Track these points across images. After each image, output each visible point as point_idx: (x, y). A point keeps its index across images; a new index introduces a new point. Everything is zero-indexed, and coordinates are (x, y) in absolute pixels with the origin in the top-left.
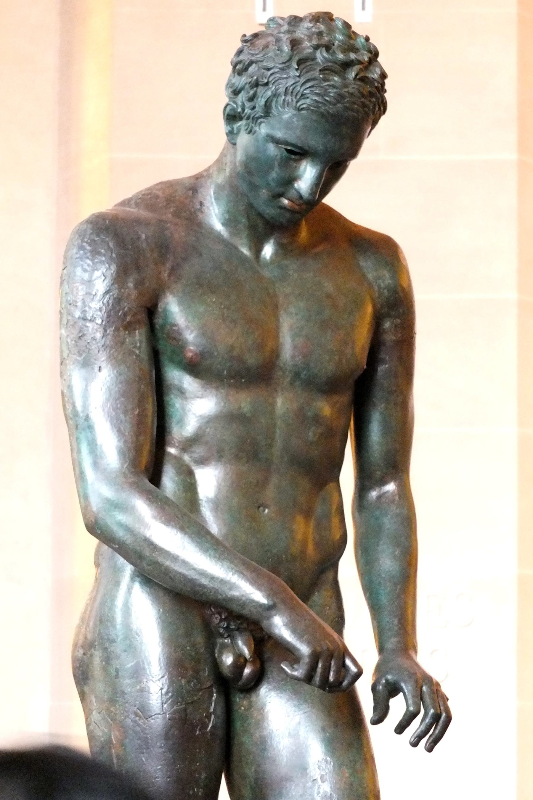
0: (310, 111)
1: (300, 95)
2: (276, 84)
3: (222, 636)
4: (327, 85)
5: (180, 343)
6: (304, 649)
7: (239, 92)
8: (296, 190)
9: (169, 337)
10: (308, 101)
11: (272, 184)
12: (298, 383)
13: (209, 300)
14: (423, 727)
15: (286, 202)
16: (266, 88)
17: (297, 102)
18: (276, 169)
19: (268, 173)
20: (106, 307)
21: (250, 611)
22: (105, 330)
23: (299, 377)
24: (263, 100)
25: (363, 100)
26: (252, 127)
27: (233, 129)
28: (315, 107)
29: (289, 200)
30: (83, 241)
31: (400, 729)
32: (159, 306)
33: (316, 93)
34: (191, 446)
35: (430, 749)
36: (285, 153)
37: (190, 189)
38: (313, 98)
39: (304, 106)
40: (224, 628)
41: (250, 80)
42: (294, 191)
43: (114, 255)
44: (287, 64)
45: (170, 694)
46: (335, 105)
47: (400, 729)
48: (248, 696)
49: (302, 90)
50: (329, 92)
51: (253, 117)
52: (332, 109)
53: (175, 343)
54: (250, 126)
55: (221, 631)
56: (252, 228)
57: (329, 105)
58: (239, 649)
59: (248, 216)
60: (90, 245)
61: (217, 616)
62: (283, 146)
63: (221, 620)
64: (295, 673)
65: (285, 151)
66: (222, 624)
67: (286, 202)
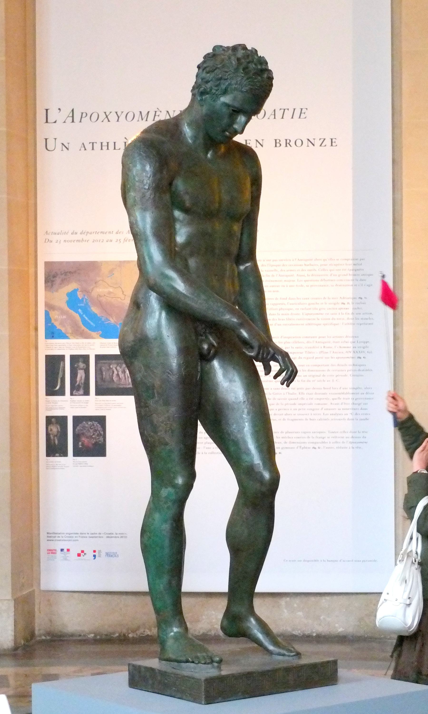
3: (202, 336)
6: (255, 344)
7: (209, 82)
8: (234, 128)
14: (287, 376)
15: (227, 133)
31: (275, 377)
35: (288, 386)
39: (245, 90)
45: (185, 364)
46: (259, 90)
47: (275, 377)
49: (245, 83)
55: (202, 333)
63: (202, 329)
64: (252, 354)
67: (227, 133)
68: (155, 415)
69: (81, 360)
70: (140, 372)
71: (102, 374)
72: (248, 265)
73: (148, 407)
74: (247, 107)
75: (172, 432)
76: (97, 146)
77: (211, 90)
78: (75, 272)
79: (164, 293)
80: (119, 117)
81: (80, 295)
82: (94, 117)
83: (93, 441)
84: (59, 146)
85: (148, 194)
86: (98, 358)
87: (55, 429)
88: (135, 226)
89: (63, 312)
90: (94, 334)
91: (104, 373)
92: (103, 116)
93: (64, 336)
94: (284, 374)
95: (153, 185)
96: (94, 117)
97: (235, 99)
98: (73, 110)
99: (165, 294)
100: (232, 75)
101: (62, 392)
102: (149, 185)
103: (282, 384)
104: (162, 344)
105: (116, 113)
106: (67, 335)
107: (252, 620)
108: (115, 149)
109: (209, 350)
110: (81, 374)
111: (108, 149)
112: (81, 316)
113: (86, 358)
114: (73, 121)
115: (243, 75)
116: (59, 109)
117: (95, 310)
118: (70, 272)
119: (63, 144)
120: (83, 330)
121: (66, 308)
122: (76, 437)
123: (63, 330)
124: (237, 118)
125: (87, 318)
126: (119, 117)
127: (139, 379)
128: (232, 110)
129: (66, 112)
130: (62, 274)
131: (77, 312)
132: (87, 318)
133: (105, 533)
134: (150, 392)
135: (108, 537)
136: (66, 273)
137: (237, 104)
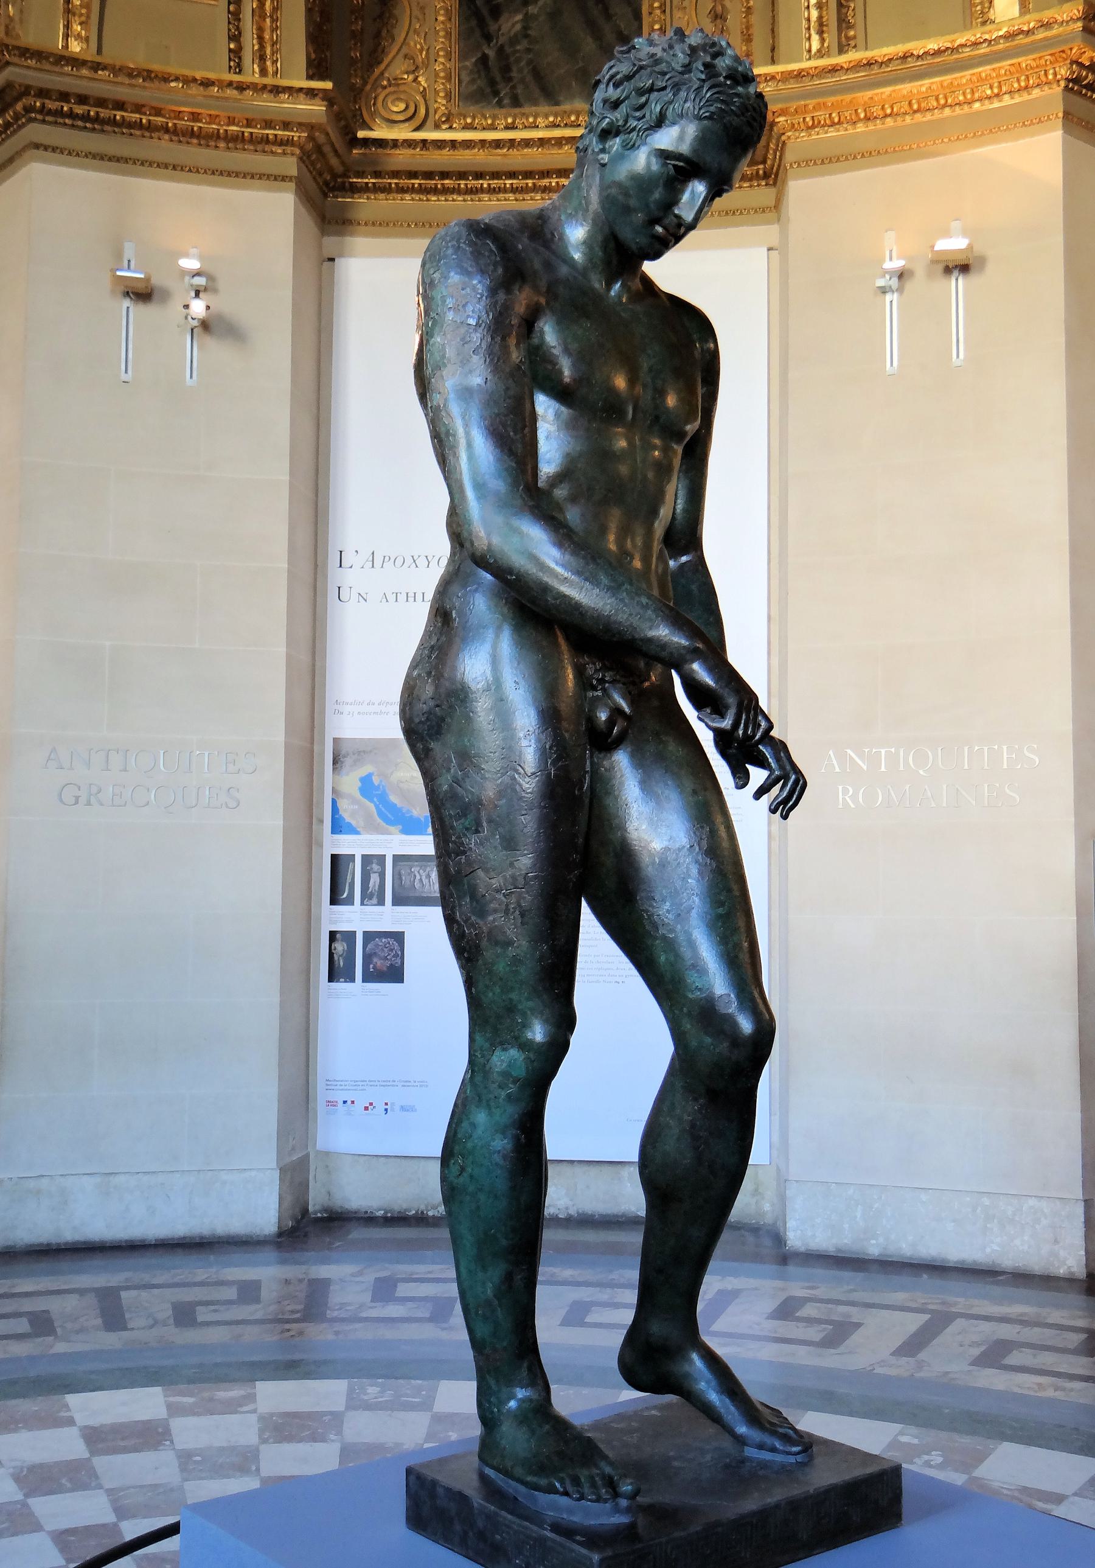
3: (594, 688)
7: (623, 101)
8: (678, 217)
11: (652, 206)
14: (785, 794)
17: (700, 109)
18: (660, 189)
19: (651, 192)
21: (671, 653)
22: (493, 338)
29: (664, 228)
30: (458, 241)
31: (759, 794)
35: (785, 817)
36: (672, 171)
39: (707, 114)
40: (598, 680)
41: (642, 85)
42: (673, 218)
43: (498, 259)
44: (688, 68)
46: (738, 116)
47: (759, 794)
48: (609, 755)
49: (708, 95)
52: (736, 121)
54: (633, 141)
55: (595, 682)
56: (607, 263)
58: (614, 702)
59: (605, 248)
60: (470, 246)
61: (590, 666)
62: (673, 162)
63: (596, 671)
66: (596, 676)
68: (480, 873)
69: (375, 861)
70: (449, 770)
71: (400, 879)
72: (684, 559)
73: (464, 853)
74: (712, 159)
75: (522, 915)
76: (402, 598)
77: (626, 121)
78: (371, 751)
79: (510, 571)
80: (429, 562)
81: (376, 780)
82: (399, 562)
83: (388, 963)
84: (355, 596)
85: (476, 337)
86: (397, 859)
87: (340, 947)
88: (443, 413)
89: (355, 801)
90: (392, 829)
91: (404, 878)
92: (409, 561)
93: (353, 831)
94: (776, 790)
95: (488, 315)
96: (399, 562)
97: (681, 138)
98: (373, 553)
99: (511, 575)
100: (676, 80)
101: (350, 901)
102: (479, 318)
103: (773, 811)
104: (502, 700)
105: (426, 557)
106: (358, 829)
107: (695, 1357)
108: (423, 600)
109: (611, 722)
110: (374, 879)
111: (415, 601)
112: (377, 806)
113: (381, 859)
114: (373, 567)
115: (703, 77)
116: (357, 551)
117: (393, 799)
118: (364, 752)
119: (359, 594)
120: (379, 824)
121: (358, 795)
122: (367, 958)
123: (354, 823)
124: (682, 191)
125: (383, 809)
126: (429, 562)
127: (445, 787)
128: (674, 166)
129: (365, 555)
130: (354, 754)
131: (372, 801)
132: (383, 809)
133: (400, 1081)
134: (471, 817)
135: (403, 1086)
136: (359, 752)
137: (685, 148)
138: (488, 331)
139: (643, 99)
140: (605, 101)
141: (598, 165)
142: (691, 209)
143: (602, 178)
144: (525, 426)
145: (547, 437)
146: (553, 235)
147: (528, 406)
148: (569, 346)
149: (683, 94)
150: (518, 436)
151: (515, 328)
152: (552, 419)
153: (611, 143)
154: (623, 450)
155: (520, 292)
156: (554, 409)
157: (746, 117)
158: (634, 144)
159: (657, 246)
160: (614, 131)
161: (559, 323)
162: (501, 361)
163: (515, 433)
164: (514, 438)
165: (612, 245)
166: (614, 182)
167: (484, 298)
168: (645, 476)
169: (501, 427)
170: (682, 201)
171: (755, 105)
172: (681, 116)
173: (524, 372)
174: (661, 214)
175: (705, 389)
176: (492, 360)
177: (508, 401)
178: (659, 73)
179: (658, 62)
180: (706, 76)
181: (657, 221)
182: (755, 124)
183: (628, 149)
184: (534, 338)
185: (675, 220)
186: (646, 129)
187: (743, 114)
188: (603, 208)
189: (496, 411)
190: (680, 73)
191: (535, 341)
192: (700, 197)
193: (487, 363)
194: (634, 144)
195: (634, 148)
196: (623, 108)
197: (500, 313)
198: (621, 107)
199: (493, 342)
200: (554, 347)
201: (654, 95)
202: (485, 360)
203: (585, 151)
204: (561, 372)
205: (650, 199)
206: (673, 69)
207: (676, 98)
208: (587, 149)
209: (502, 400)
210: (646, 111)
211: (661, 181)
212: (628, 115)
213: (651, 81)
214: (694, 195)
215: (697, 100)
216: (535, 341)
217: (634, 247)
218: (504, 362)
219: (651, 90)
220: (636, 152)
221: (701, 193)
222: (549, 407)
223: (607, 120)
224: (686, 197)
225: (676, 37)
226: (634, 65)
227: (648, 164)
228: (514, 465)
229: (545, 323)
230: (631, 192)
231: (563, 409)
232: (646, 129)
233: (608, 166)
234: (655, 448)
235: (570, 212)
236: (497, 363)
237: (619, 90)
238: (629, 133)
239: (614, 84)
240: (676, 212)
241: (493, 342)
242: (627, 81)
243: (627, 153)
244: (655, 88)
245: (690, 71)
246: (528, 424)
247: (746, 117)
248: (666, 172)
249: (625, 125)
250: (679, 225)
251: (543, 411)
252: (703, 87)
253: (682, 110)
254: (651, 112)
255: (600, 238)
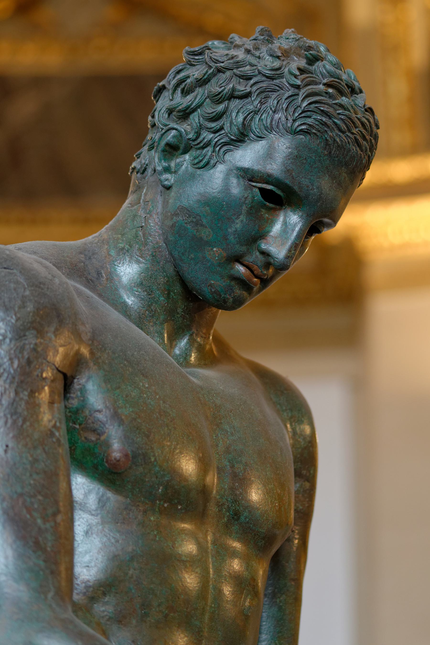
0: (308, 137)
1: (300, 112)
2: (263, 95)
4: (336, 104)
5: (102, 438)
7: (194, 110)
8: (264, 253)
9: (86, 429)
10: (309, 121)
11: (231, 238)
12: (236, 528)
13: (141, 384)
15: (241, 269)
16: (247, 101)
17: (294, 121)
20: (19, 361)
22: (17, 393)
23: (239, 518)
24: (240, 114)
25: (370, 137)
26: (210, 158)
27: (169, 166)
28: (319, 131)
32: (76, 381)
33: (322, 111)
34: (104, 594)
36: (258, 196)
37: (81, 253)
38: (319, 118)
39: (303, 127)
41: (220, 90)
42: (258, 253)
44: (278, 72)
46: (343, 132)
50: (339, 114)
51: (216, 142)
53: (93, 438)
54: (207, 157)
57: (337, 131)
59: (169, 294)
65: (259, 192)
95: (12, 363)
100: (264, 85)
124: (272, 223)
128: (261, 190)
138: (11, 383)
139: (221, 107)
140: (170, 111)
141: (160, 188)
142: (283, 244)
143: (165, 203)
144: (59, 512)
145: (87, 533)
146: (99, 274)
147: (63, 485)
148: (120, 411)
149: (272, 102)
150: (48, 525)
151: (48, 382)
152: (93, 507)
153: (178, 160)
154: (190, 555)
155: (56, 336)
156: (98, 493)
157: (353, 133)
158: (208, 163)
159: (238, 292)
160: (182, 147)
161: (107, 380)
162: (28, 423)
163: (45, 520)
164: (43, 526)
165: (178, 288)
166: (182, 209)
167: (8, 340)
168: (220, 592)
169: (25, 511)
170: (272, 234)
171: (364, 120)
172: (270, 129)
173: (58, 440)
174: (244, 248)
175: (298, 485)
176: (14, 422)
177: (35, 476)
178: (241, 77)
179: (239, 64)
180: (302, 81)
181: (238, 259)
182: (365, 143)
183: (199, 168)
184: (73, 398)
185: (260, 257)
186: (226, 144)
187: (349, 131)
188: (166, 241)
189: (19, 490)
190: (267, 77)
191: (74, 403)
192: (293, 230)
193: (9, 424)
194: (208, 163)
195: (208, 167)
196: (195, 118)
197: (29, 362)
198: (191, 117)
199: (17, 399)
200: (99, 411)
201: (235, 104)
202: (6, 423)
203: (143, 173)
204: (107, 445)
205: (229, 230)
206: (260, 73)
207: (264, 106)
208: (145, 169)
209: (28, 474)
210: (225, 121)
211: (244, 207)
212: (200, 126)
213: (231, 86)
214: (286, 226)
215: (291, 110)
216: (74, 403)
217: (206, 290)
218: (31, 425)
219: (232, 96)
220: (212, 171)
221: (295, 225)
222: (90, 491)
223: (173, 132)
224: (277, 228)
225: (262, 37)
226: (210, 67)
227: (226, 187)
228: (42, 563)
229: (89, 378)
230: (204, 221)
231: (109, 494)
232: (226, 144)
233: (174, 189)
234: (234, 554)
235: (121, 245)
236: (22, 426)
237: (189, 97)
238: (203, 148)
239: (183, 91)
240: (263, 246)
241: (17, 399)
242: (200, 86)
243: (199, 172)
244: (237, 93)
245: (281, 76)
246: (62, 509)
247: (353, 133)
248: (250, 196)
249: (197, 138)
250: (268, 265)
251: (81, 497)
252: (298, 95)
253: (271, 121)
254: (231, 123)
255: (162, 280)
